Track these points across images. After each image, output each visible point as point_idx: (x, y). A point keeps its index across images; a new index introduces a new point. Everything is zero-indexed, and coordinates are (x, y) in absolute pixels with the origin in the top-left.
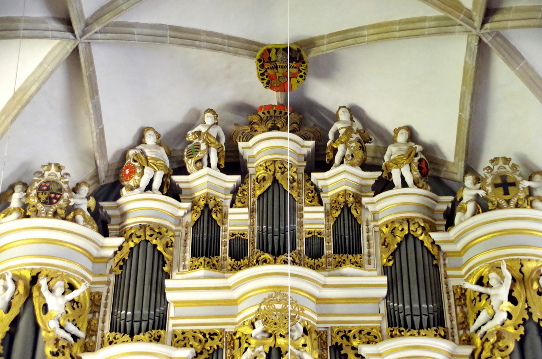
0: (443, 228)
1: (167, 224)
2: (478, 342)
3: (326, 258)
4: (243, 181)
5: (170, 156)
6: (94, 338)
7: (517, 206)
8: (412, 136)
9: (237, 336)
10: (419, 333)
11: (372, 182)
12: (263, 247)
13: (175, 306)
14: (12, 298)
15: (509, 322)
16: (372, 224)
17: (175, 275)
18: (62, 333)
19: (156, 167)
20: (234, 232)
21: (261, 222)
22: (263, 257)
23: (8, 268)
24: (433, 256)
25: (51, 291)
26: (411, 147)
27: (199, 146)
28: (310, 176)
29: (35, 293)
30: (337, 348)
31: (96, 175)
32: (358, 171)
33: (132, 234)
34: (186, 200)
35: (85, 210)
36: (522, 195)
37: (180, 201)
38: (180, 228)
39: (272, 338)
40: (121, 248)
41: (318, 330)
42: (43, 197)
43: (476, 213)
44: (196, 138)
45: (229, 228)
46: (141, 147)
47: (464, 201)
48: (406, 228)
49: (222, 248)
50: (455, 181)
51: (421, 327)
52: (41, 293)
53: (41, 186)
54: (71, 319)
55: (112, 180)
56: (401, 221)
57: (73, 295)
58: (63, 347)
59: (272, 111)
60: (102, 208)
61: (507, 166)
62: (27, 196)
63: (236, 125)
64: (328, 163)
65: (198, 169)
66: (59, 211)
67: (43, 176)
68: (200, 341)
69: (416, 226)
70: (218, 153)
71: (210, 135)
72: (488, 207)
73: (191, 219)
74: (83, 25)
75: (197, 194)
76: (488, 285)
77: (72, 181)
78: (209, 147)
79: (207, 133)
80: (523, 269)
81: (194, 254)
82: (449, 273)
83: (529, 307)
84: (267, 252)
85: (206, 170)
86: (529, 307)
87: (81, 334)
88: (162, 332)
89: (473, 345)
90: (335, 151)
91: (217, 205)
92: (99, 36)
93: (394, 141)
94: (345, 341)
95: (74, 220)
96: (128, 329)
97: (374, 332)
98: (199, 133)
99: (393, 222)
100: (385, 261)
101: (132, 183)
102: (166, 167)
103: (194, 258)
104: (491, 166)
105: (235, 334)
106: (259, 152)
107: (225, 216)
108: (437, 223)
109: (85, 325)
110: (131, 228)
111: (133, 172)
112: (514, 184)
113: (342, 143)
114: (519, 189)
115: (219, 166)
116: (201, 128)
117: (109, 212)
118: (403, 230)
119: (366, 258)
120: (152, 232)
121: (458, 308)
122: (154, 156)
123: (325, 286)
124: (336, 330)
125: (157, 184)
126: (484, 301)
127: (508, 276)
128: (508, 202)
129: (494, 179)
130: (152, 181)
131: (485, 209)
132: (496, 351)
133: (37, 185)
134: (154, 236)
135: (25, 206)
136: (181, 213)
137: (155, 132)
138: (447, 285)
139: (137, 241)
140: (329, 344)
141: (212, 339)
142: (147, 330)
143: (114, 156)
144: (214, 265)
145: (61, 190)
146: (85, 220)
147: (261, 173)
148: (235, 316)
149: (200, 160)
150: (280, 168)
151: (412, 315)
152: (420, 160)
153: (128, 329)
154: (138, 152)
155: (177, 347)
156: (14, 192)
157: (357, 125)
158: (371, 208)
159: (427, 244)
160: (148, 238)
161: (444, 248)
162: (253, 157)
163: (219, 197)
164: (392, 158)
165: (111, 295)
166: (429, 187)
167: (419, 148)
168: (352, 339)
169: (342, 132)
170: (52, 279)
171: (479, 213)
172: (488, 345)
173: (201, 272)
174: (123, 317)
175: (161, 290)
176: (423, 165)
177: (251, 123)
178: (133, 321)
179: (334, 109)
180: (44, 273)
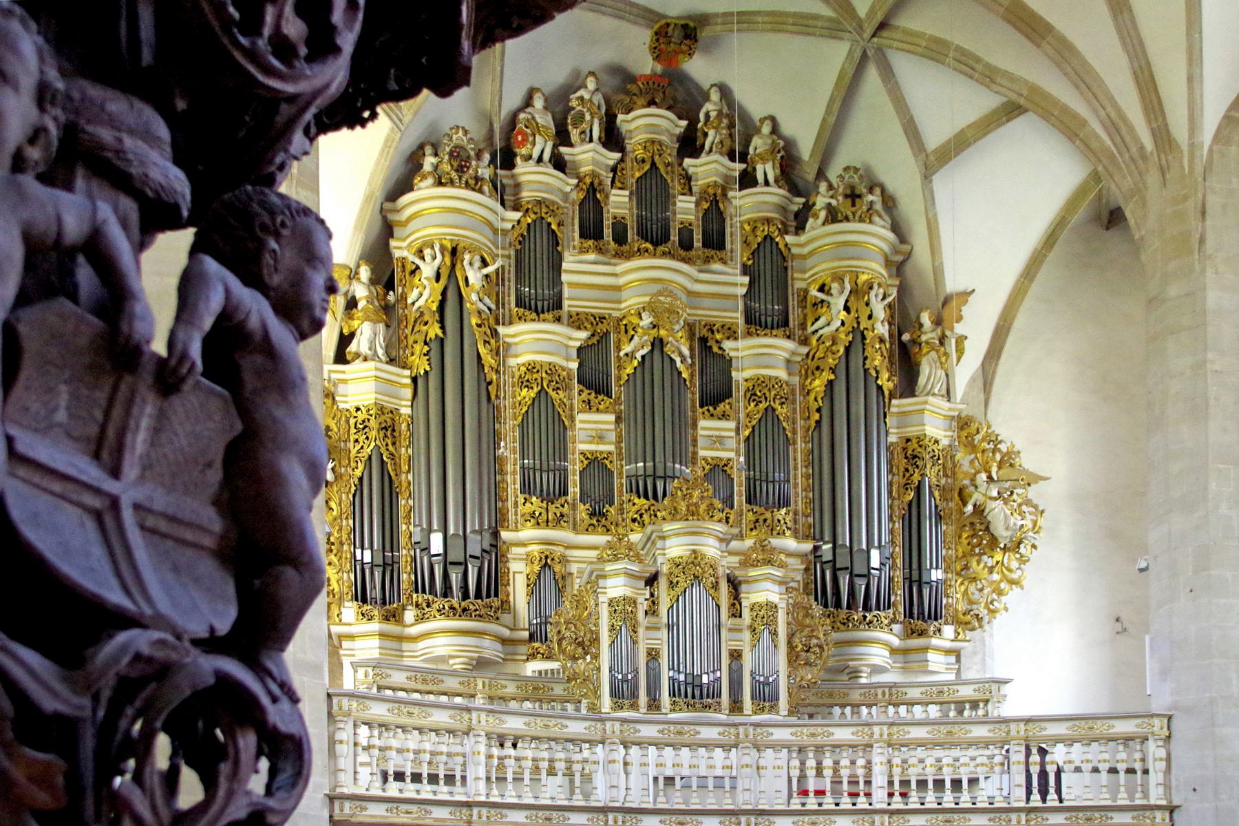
0: (793, 229)
2: (814, 342)
4: (622, 160)
8: (775, 130)
12: (643, 234)
15: (842, 329)
30: (703, 340)
40: (519, 222)
45: (611, 210)
46: (529, 110)
49: (605, 230)
51: (772, 328)
57: (486, 271)
68: (592, 324)
73: (577, 196)
76: (829, 293)
79: (590, 100)
82: (795, 275)
84: (647, 240)
87: (493, 307)
90: (706, 135)
94: (710, 333)
95: (480, 191)
96: (533, 307)
98: (582, 98)
99: (755, 221)
101: (524, 151)
103: (583, 240)
105: (621, 320)
106: (637, 128)
107: (607, 197)
110: (528, 202)
111: (525, 140)
113: (714, 128)
115: (600, 138)
119: (729, 254)
123: (697, 281)
125: (547, 156)
130: (542, 152)
132: (829, 354)
136: (568, 189)
147: (640, 153)
148: (620, 302)
152: (782, 157)
153: (533, 307)
158: (736, 202)
159: (781, 246)
160: (543, 215)
161: (795, 250)
165: (513, 269)
167: (782, 143)
168: (716, 333)
169: (713, 114)
173: (592, 256)
174: (527, 294)
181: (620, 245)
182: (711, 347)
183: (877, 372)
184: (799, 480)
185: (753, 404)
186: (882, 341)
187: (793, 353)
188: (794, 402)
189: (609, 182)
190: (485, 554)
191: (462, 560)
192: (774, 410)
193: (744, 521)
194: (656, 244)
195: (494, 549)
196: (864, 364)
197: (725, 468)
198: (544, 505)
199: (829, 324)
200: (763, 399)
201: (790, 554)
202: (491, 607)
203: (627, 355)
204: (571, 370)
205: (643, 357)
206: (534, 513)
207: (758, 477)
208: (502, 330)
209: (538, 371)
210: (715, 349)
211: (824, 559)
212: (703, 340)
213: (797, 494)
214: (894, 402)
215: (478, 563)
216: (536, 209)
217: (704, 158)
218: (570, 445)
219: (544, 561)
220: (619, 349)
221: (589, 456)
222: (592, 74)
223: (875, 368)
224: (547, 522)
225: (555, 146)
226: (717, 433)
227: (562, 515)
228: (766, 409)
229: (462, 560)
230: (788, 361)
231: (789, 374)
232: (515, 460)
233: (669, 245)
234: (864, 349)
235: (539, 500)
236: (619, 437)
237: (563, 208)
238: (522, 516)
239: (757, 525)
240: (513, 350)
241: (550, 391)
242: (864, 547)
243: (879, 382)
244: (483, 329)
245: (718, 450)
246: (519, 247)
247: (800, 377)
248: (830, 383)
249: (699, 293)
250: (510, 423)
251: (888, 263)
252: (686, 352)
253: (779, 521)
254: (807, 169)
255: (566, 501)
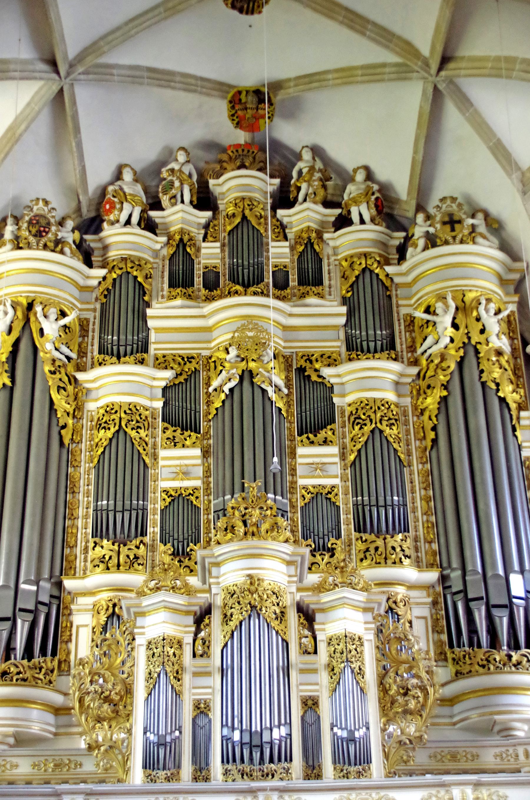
0: (396, 261)
1: (146, 256)
2: (424, 363)
3: (291, 289)
4: (214, 217)
5: (146, 192)
6: (84, 359)
7: (462, 242)
8: (370, 176)
9: (213, 360)
10: (374, 357)
11: (333, 219)
12: (234, 279)
13: (156, 333)
14: (12, 322)
15: (451, 345)
16: (332, 259)
17: (154, 304)
18: (57, 354)
19: (134, 202)
20: (209, 265)
21: (231, 256)
22: (234, 288)
23: (6, 295)
24: (387, 288)
25: (45, 317)
26: (368, 186)
27: (173, 183)
28: (276, 212)
29: (32, 319)
30: (301, 370)
31: (79, 209)
32: (320, 208)
33: (114, 266)
34: (162, 235)
35: (71, 243)
36: (466, 232)
37: (156, 234)
38: (157, 261)
39: (244, 362)
40: (104, 278)
41: (285, 354)
42: (34, 231)
43: (426, 248)
44: (170, 175)
45: (202, 261)
46: (119, 183)
47: (416, 237)
48: (363, 262)
50: (407, 218)
51: (376, 351)
52: (37, 318)
53: (31, 220)
54: (65, 342)
55: (93, 214)
56: (360, 255)
58: (59, 366)
59: (240, 150)
60: (86, 241)
61: (453, 205)
62: (19, 229)
63: (207, 162)
64: (292, 200)
65: (174, 204)
66: (49, 244)
67: (32, 210)
68: (179, 364)
69: (373, 260)
70: (191, 190)
71: (183, 173)
72: (436, 242)
73: (167, 252)
74: (67, 66)
75: (172, 229)
76: (435, 313)
77: (58, 214)
78: (182, 184)
79: (180, 171)
80: (465, 299)
81: (171, 285)
82: (401, 302)
83: (468, 332)
85: (180, 206)
86: (468, 332)
87: (74, 355)
88: (145, 355)
89: (419, 365)
90: (299, 189)
91: (190, 239)
92: (82, 77)
93: (352, 180)
94: (308, 365)
95: (62, 252)
96: (115, 352)
97: (334, 356)
98: (172, 170)
99: (352, 257)
100: (344, 292)
101: (112, 217)
102: (143, 203)
103: (172, 289)
104: (440, 205)
105: (210, 358)
106: (229, 190)
107: (198, 250)
108: (391, 257)
109: (76, 347)
110: (113, 260)
111: (113, 207)
112: (459, 222)
113: (305, 181)
114: (463, 226)
115: (191, 202)
116: (174, 165)
117: (92, 245)
118: (360, 264)
119: (327, 289)
120: (132, 265)
121: (408, 334)
122: (132, 192)
123: (291, 315)
124: (300, 354)
125: (135, 219)
126: (430, 328)
127: (452, 305)
128: (454, 238)
129: (442, 217)
130: (130, 216)
131: (434, 245)
132: (439, 371)
133: (27, 218)
134: (135, 268)
135: (17, 238)
136: (158, 246)
137: (132, 169)
138: (398, 313)
139: (119, 272)
140: (295, 367)
141: (190, 362)
142: (132, 353)
143: (94, 193)
144: (189, 295)
145: (49, 224)
146: (72, 252)
147: (231, 210)
148: (210, 342)
149: (174, 197)
150: (249, 205)
151: (368, 341)
152: (377, 199)
153: (115, 352)
154: (117, 188)
155: (159, 369)
156: (6, 225)
157: (319, 165)
158: (332, 243)
159: (382, 277)
160: (129, 270)
161: (397, 280)
162: (223, 194)
163: (192, 232)
164: (351, 196)
166: (384, 224)
167: (376, 187)
168: (314, 362)
169: (305, 171)
170: (46, 306)
171: (428, 248)
172: (432, 366)
173: (178, 302)
174: (110, 342)
175: (144, 318)
176: (379, 203)
177: (220, 162)
178: (119, 345)
179: (298, 149)
180: (38, 300)
181: (211, 290)
182: (309, 376)
183: (498, 385)
184: (418, 503)
185: (357, 428)
186: (499, 353)
187: (402, 375)
188: (406, 423)
189: (201, 237)
190: (40, 607)
191: (10, 614)
192: (381, 432)
193: (353, 552)
194: (246, 286)
195: (55, 602)
196: (480, 377)
197: (329, 496)
198: (116, 547)
199: (437, 342)
200: (368, 422)
201: (411, 587)
202: (41, 669)
203: (215, 390)
204: (155, 409)
205: (231, 390)
206: (104, 557)
207: (366, 502)
208: (80, 376)
209: (116, 412)
210: (314, 378)
211: (454, 590)
212: (301, 370)
213: (416, 520)
214: (523, 414)
215: (30, 617)
216: (122, 265)
217: (297, 208)
218: (151, 484)
219: (111, 610)
220: (208, 385)
221: (173, 493)
222: (183, 149)
223: (494, 381)
224: (119, 565)
225: (142, 211)
226: (317, 460)
227: (136, 557)
228: (372, 431)
229: (10, 614)
230: (397, 383)
231: (399, 395)
232: (89, 503)
233: (261, 286)
234: (479, 363)
235: (110, 543)
236: (207, 473)
237: (151, 263)
238: (92, 561)
239: (368, 554)
240: (93, 395)
241: (128, 430)
242: (501, 572)
243: (501, 394)
244: (58, 376)
245: (320, 477)
246: (104, 300)
247: (412, 398)
248: (444, 400)
249: (295, 327)
250: (84, 466)
251: (503, 282)
252: (281, 383)
253: (393, 548)
254: (405, 207)
255: (141, 542)
